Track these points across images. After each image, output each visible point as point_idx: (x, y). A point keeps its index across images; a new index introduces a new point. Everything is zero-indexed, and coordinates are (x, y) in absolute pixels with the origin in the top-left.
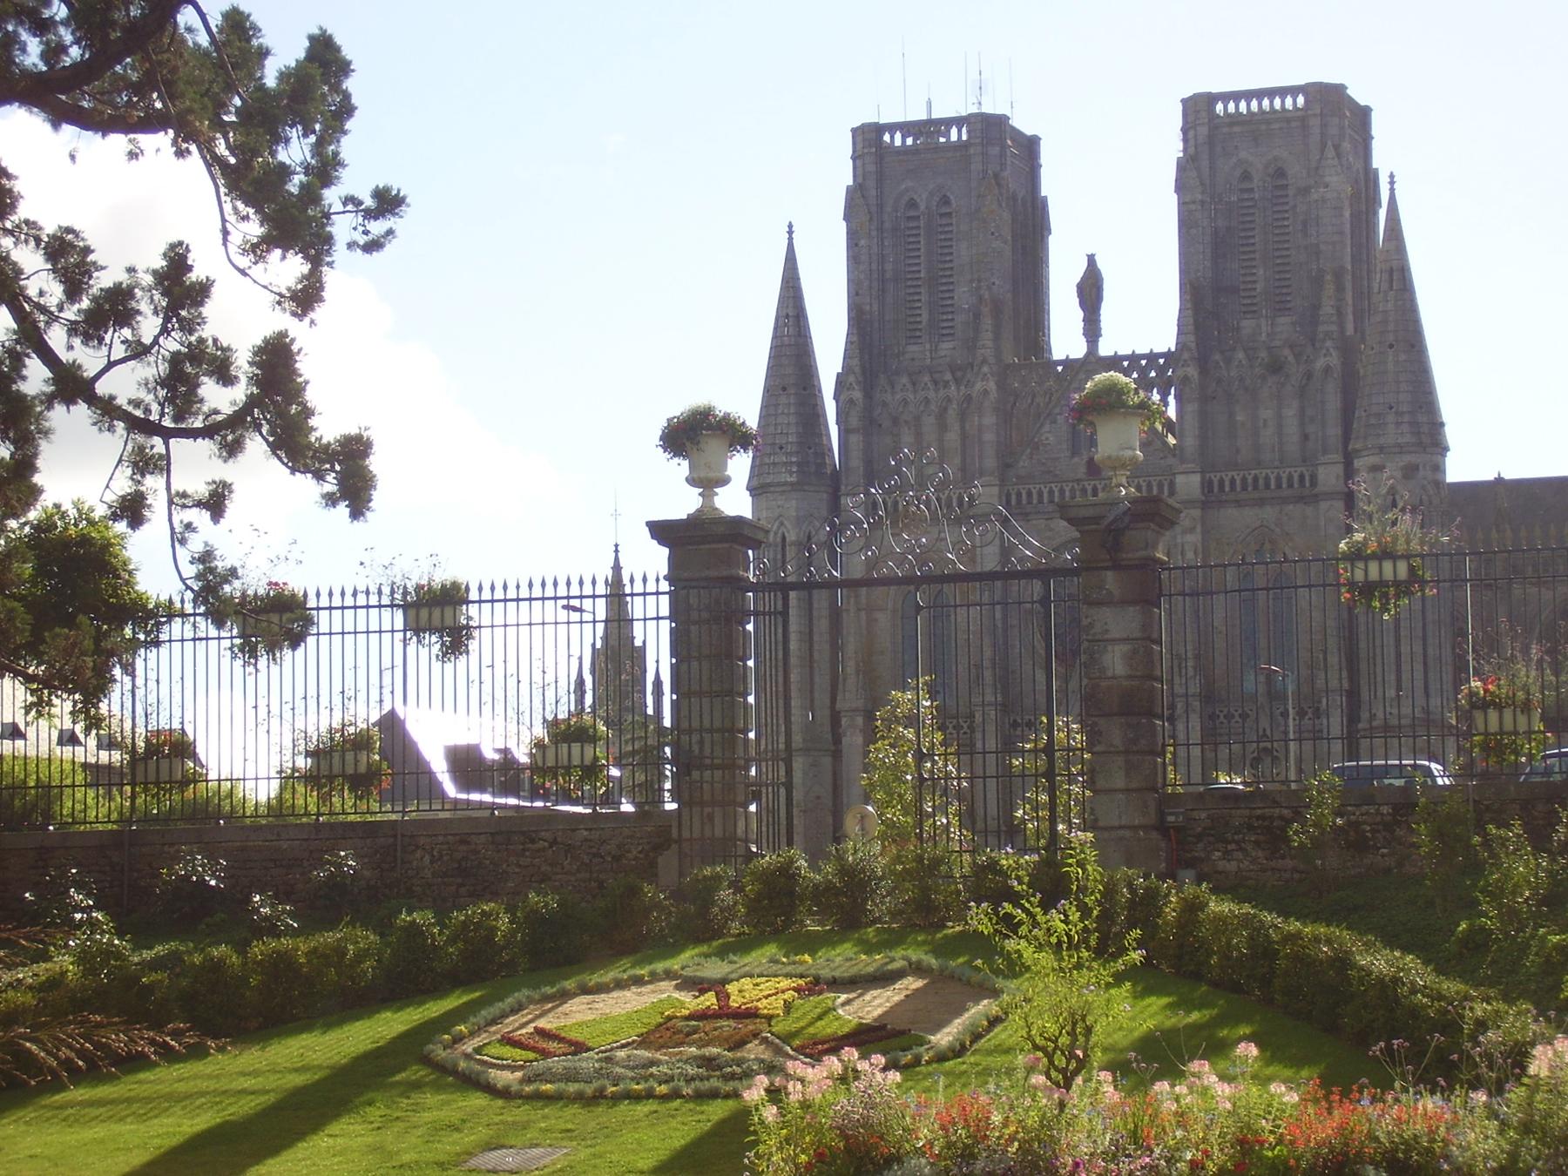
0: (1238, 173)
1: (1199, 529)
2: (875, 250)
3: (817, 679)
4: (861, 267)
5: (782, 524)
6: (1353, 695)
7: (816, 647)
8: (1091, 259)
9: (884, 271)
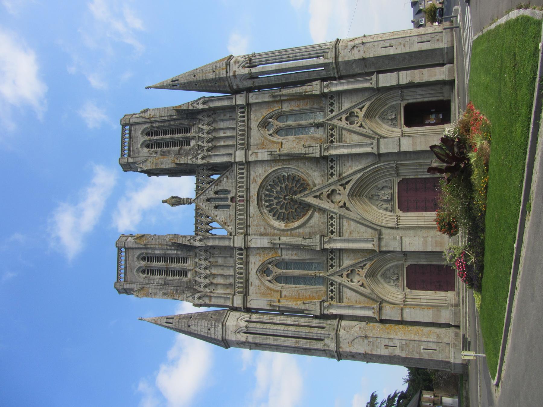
3: (306, 324)
4: (158, 292)
6: (323, 80)
7: (292, 323)
8: (165, 201)
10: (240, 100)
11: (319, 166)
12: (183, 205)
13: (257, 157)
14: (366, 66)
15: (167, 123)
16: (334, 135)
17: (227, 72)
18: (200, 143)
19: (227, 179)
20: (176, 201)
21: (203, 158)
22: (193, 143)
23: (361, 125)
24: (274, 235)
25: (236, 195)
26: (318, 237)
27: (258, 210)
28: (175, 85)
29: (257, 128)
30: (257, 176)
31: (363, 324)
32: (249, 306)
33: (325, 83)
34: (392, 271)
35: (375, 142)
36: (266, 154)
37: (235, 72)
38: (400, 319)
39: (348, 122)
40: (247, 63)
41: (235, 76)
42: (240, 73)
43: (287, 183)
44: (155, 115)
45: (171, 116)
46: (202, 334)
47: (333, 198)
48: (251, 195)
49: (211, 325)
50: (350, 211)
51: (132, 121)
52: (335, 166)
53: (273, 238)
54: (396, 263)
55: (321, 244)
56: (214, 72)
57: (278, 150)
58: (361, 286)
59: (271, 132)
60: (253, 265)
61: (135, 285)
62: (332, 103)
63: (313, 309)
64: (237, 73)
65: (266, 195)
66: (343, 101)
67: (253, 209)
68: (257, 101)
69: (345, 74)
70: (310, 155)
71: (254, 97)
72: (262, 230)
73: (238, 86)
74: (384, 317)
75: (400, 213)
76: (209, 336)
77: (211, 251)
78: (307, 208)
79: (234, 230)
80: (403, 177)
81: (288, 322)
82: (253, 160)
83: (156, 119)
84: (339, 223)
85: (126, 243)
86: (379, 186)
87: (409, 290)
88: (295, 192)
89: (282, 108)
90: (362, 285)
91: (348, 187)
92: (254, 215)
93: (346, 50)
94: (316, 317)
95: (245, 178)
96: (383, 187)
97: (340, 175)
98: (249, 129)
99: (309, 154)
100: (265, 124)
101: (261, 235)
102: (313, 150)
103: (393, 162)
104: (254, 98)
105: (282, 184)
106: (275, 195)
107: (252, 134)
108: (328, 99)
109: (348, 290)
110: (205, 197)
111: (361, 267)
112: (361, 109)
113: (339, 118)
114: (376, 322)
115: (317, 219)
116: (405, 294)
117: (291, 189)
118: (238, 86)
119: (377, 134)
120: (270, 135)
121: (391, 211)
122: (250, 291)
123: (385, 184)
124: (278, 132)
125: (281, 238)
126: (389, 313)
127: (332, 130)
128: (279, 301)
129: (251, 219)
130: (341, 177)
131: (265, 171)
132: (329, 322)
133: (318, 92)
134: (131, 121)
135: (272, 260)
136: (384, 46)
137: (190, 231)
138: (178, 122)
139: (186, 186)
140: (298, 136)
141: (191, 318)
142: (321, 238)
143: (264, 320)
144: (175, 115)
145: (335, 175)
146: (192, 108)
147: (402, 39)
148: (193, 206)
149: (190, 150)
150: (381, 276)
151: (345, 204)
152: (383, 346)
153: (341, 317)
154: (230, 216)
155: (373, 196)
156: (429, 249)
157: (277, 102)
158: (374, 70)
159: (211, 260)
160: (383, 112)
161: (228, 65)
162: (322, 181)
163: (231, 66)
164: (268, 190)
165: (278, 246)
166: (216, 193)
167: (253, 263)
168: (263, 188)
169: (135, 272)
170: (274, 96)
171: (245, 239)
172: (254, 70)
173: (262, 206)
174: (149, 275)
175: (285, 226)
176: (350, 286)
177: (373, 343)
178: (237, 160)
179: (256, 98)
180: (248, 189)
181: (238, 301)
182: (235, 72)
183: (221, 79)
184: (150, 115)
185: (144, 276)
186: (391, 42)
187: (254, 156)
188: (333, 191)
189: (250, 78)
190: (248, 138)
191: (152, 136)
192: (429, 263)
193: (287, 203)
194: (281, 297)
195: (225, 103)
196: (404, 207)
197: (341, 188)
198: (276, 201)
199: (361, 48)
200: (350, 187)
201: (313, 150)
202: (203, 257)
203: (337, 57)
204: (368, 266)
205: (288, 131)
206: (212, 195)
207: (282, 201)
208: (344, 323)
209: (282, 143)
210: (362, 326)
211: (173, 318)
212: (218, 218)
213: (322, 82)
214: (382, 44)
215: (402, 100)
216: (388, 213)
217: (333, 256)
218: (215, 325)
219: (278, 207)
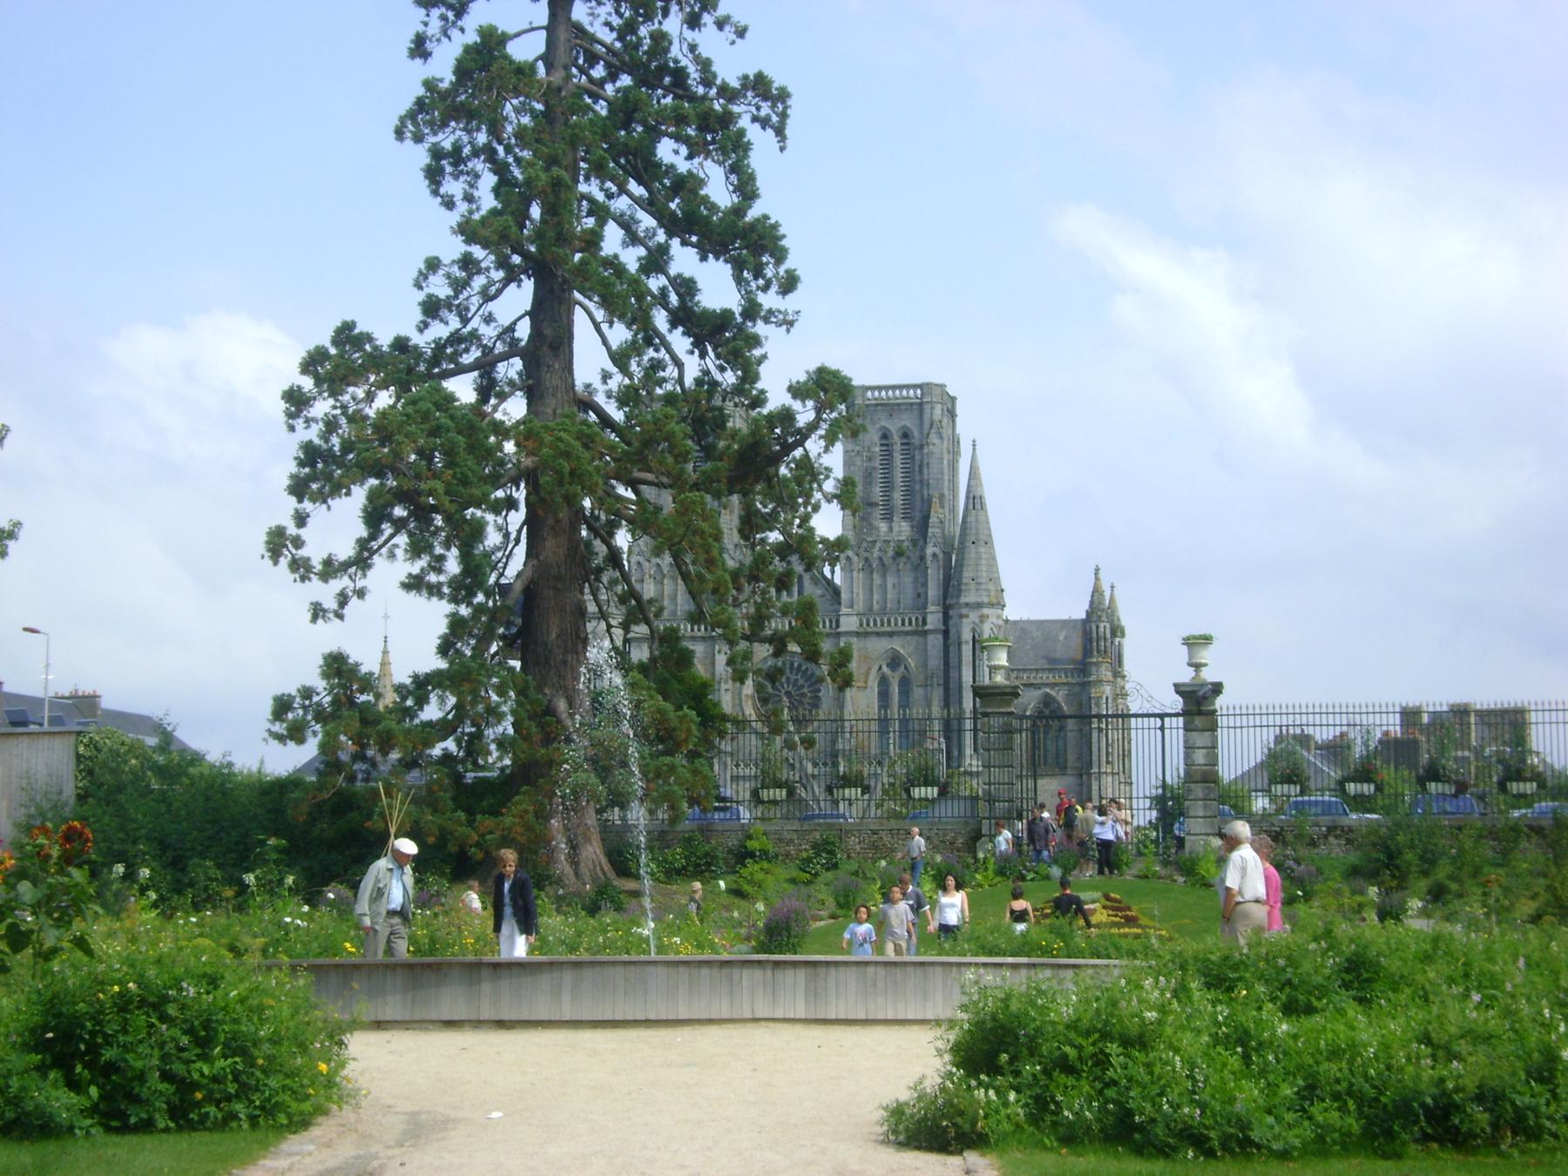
22: (883, 527)
41: (961, 616)
51: (927, 408)
65: (792, 664)
97: (813, 776)
98: (891, 634)
100: (895, 661)
104: (935, 641)
124: (884, 682)
161: (979, 605)
178: (843, 620)
205: (884, 695)
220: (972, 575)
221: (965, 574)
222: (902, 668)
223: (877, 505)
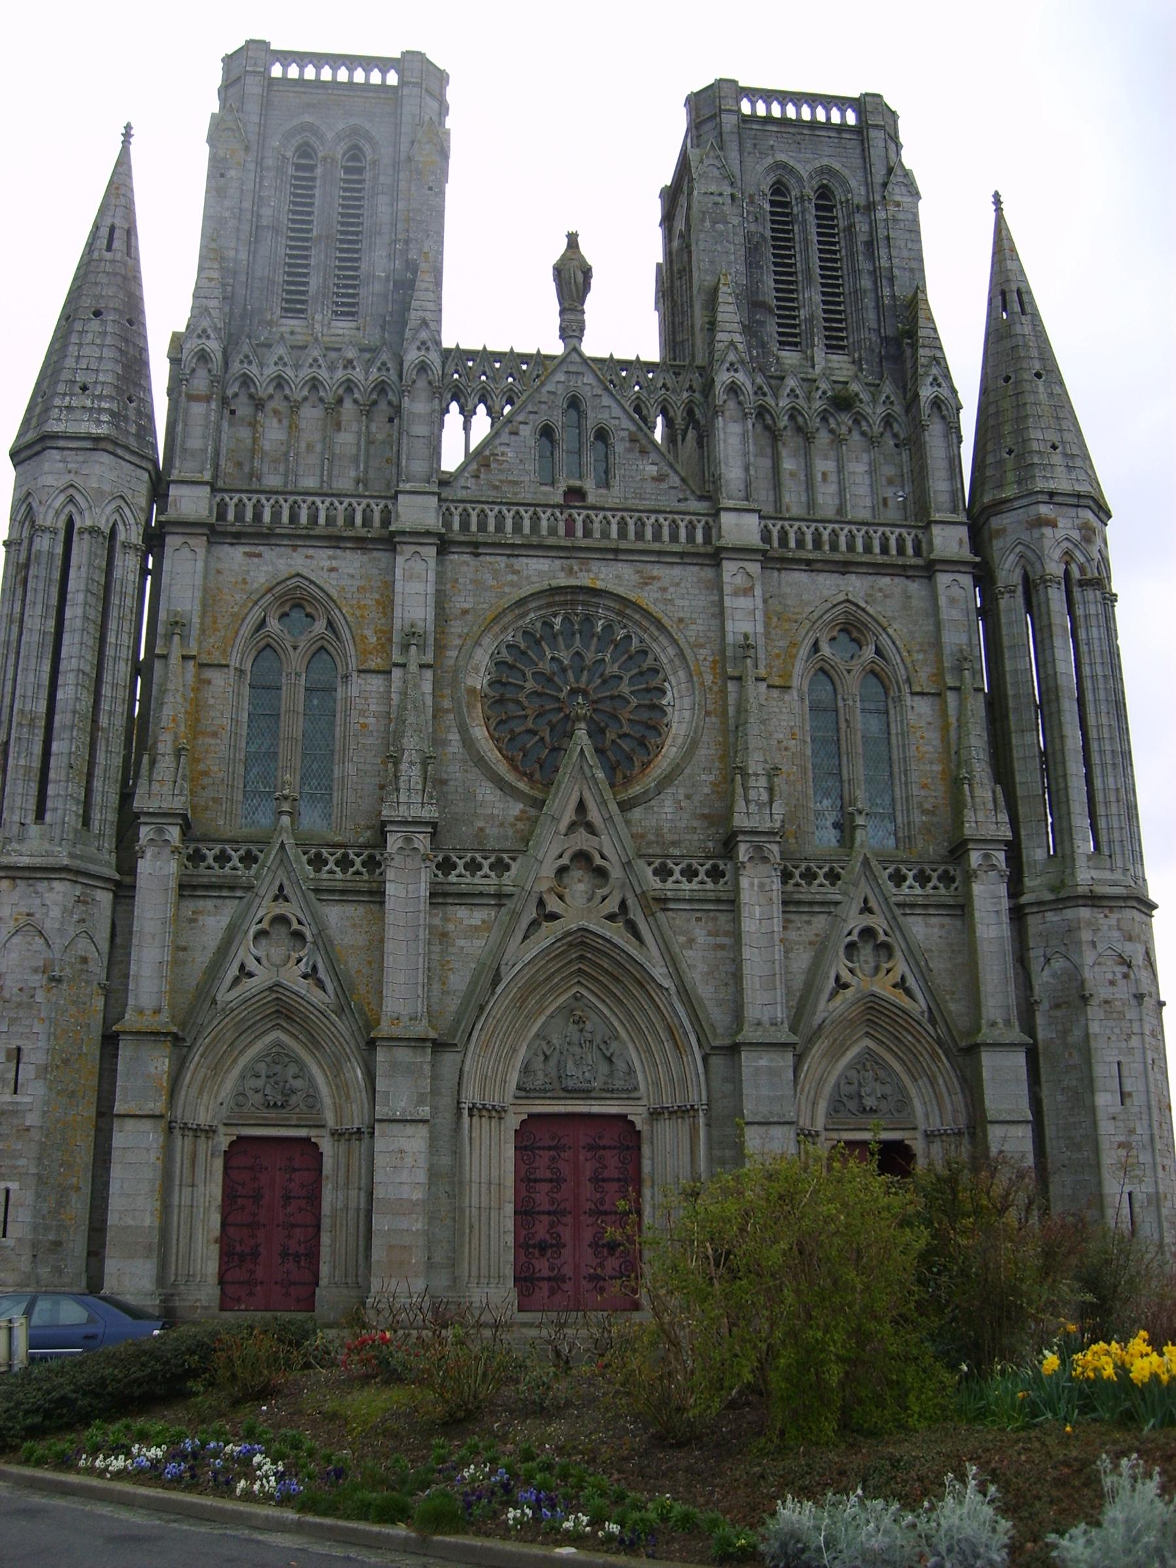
0: (771, 179)
1: (758, 591)
2: (250, 186)
3: (101, 758)
4: (227, 203)
5: (71, 500)
7: (105, 706)
8: (572, 239)
9: (259, 216)
10: (950, 540)
11: (696, 823)
12: (557, 308)
13: (736, 593)
14: (1057, 1006)
15: (865, 265)
16: (809, 884)
17: (1052, 494)
18: (791, 382)
19: (653, 479)
20: (573, 280)
21: (734, 389)
22: (790, 357)
23: (846, 986)
24: (440, 647)
25: (593, 508)
26: (429, 812)
27: (537, 587)
28: (1010, 298)
29: (842, 597)
30: (664, 590)
31: (98, 969)
32: (172, 542)
33: (1001, 856)
34: (298, 1084)
35: (784, 1036)
36: (747, 627)
37: (1053, 525)
38: (119, 1108)
39: (854, 937)
40: (1082, 570)
41: (1041, 522)
42: (1047, 543)
43: (634, 701)
44: (895, 220)
45: (891, 279)
46: (70, 362)
47: (576, 874)
48: (595, 566)
49: (100, 397)
50: (525, 938)
52: (694, 885)
53: (431, 641)
54: (327, 1101)
55: (406, 823)
56: (1054, 447)
57: (762, 672)
58: (242, 967)
59: (826, 650)
60: (326, 564)
61: (255, 118)
62: (929, 879)
63: (156, 787)
64: (1048, 531)
66: (933, 920)
67: (540, 572)
68: (943, 601)
69: (1032, 930)
70: (739, 790)
71: (956, 591)
72: (461, 601)
73: (1001, 532)
74: (126, 1051)
75: (513, 1121)
76: (61, 388)
77: (383, 406)
78: (537, 776)
79: (462, 494)
80: (645, 1135)
81: (106, 690)
82: (726, 577)
83: (881, 225)
84: (481, 894)
85: (416, 91)
86: (614, 1046)
87: (224, 1146)
88: (602, 731)
89: (913, 694)
90: (245, 972)
91: (616, 933)
92: (517, 572)
93: (1116, 934)
94: (126, 797)
95: (656, 546)
96: (609, 1060)
97: (663, 901)
98: (844, 568)
99: (746, 789)
101: (441, 600)
102: (760, 805)
103: (704, 1098)
105: (631, 684)
106: (590, 656)
107: (821, 578)
108: (941, 869)
109: (225, 921)
110: (587, 392)
111: (315, 968)
112: (901, 984)
113: (873, 903)
114: (106, 1023)
115: (494, 808)
116: (210, 1132)
117: (615, 717)
118: (1001, 532)
119: (810, 1042)
120: (816, 647)
121: (519, 1088)
122: (227, 548)
123: (620, 1065)
125: (429, 674)
126: (143, 1072)
127: (833, 877)
128: (185, 658)
129: (502, 562)
130: (655, 907)
131: (681, 620)
132: (109, 844)
133: (969, 829)
134: (873, 133)
135: (345, 634)
136: (1125, 1073)
137: (458, 332)
138: (869, 302)
139: (626, 325)
140: (809, 752)
141: (130, 322)
142: (427, 824)
143: (115, 600)
144: (893, 297)
145: (660, 885)
146: (923, 361)
147: (1146, 1138)
148: (556, 348)
149: (763, 345)
150: (278, 1043)
151: (553, 917)
152: (20, 1043)
153: (124, 891)
154: (516, 483)
155: (580, 1021)
156: (380, 1223)
157: (939, 674)
158: (1041, 1035)
159: (348, 404)
160: (886, 1067)
162: (643, 836)
163: (1072, 512)
164: (608, 628)
165: (396, 657)
166: (602, 435)
167: (334, 564)
168: (620, 613)
169: (307, 118)
170: (959, 670)
171: (428, 533)
172: (1056, 598)
173: (550, 605)
174: (291, 170)
175: (472, 691)
176: (245, 927)
177: (30, 1006)
179: (952, 601)
180: (615, 554)
181: (191, 502)
182: (1053, 525)
183: (1025, 470)
184: (898, 204)
185: (289, 154)
186: (1138, 1100)
187: (740, 580)
188: (601, 873)
189: (1026, 578)
190: (808, 562)
191: (818, 207)
192: (326, 1223)
193: (558, 699)
194: (202, 666)
195: (939, 485)
196: (534, 1136)
197: (612, 906)
198: (565, 657)
199: (1122, 992)
200: (616, 939)
201: (760, 805)
202: (358, 374)
203: (1093, 900)
204: (317, 997)
205: (825, 712)
206: (593, 419)
207: (566, 683)
208: (105, 898)
209: (786, 688)
210: (92, 967)
211: (129, 254)
212: (505, 438)
213: (1007, 843)
214: (1133, 1067)
215: (929, 1136)
216: (514, 1077)
217: (358, 865)
218: (100, 410)
219: (545, 667)
220: (1053, 436)
221: (1035, 434)
222: (869, 652)
223: (770, 310)
